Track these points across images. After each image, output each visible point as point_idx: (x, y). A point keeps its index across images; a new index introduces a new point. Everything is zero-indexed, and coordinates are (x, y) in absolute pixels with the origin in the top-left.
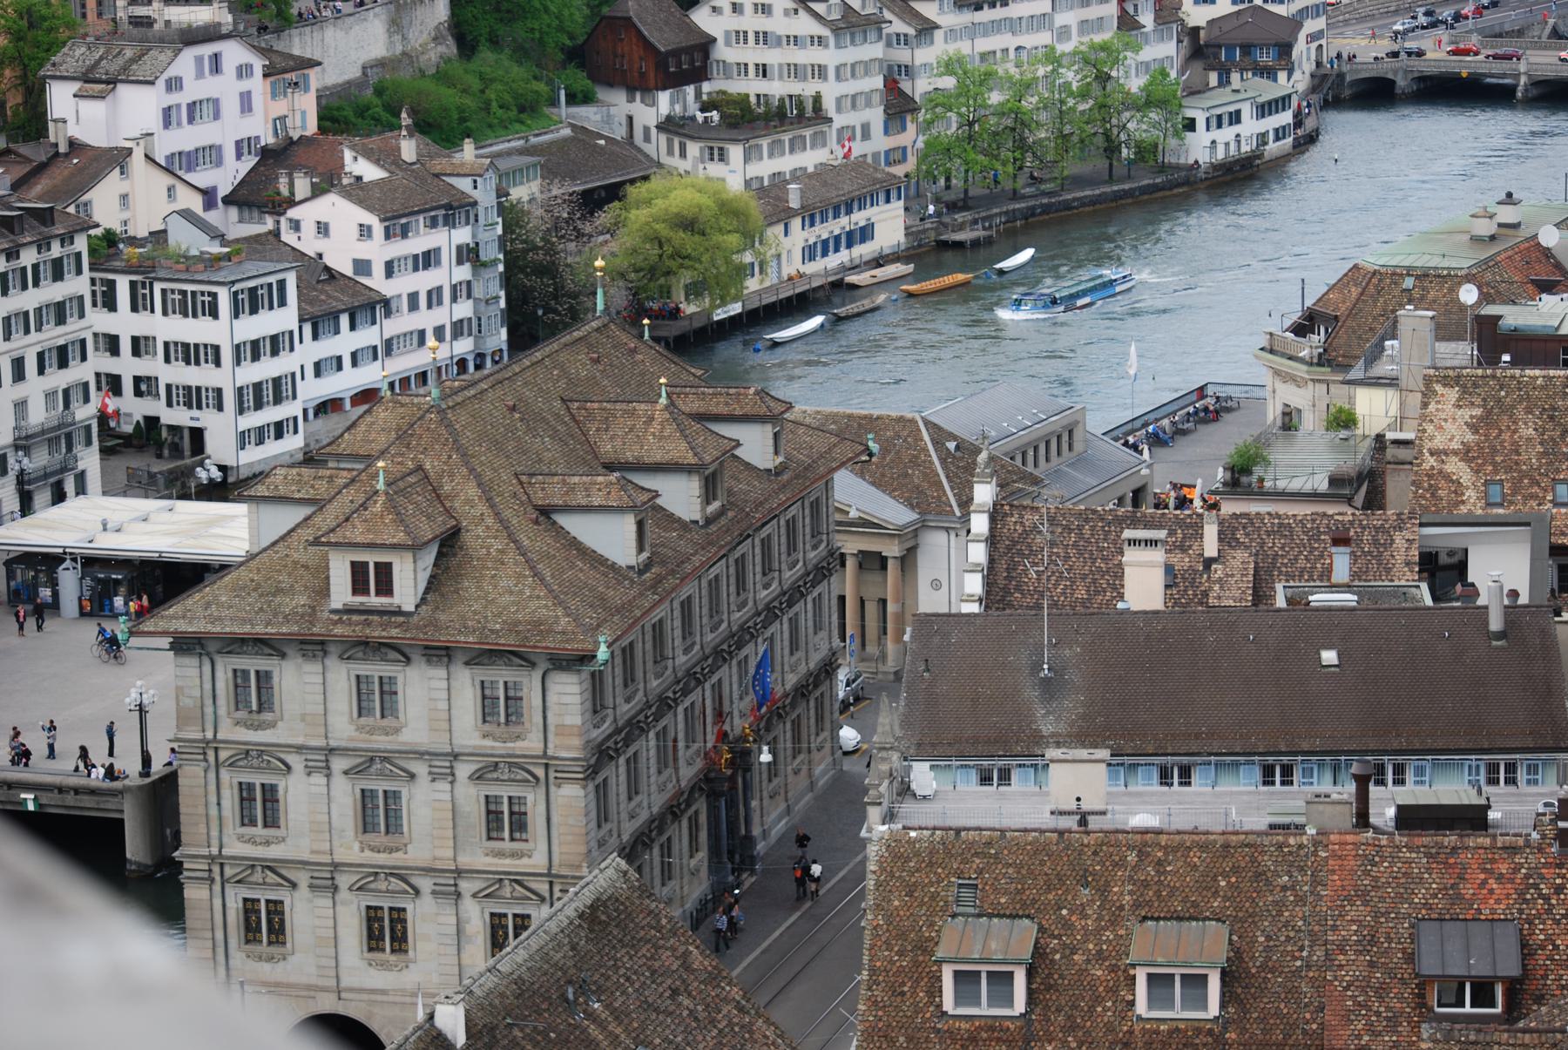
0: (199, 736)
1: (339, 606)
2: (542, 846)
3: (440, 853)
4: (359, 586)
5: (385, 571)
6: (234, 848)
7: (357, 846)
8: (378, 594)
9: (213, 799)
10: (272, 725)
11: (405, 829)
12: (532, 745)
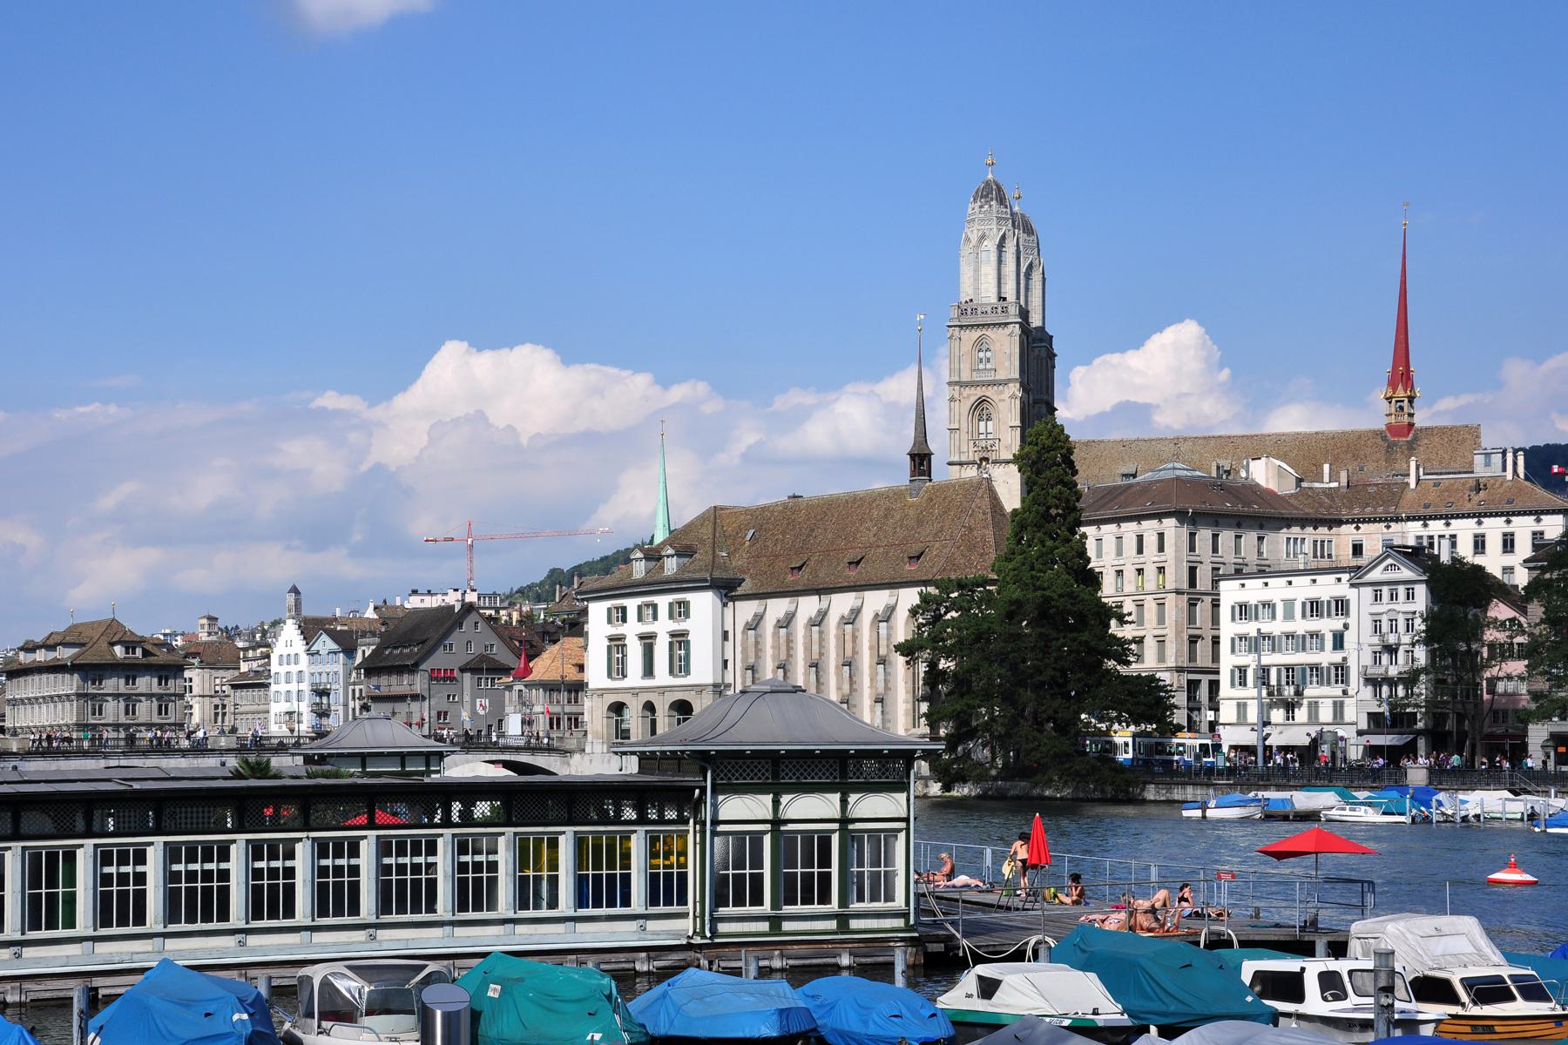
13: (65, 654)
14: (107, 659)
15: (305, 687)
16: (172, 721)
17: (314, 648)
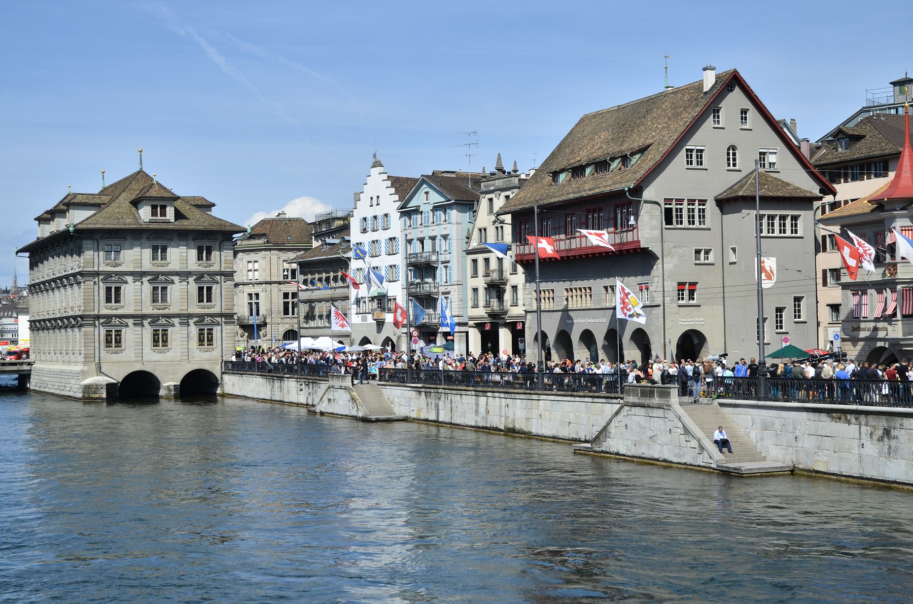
0: (91, 269)
2: (219, 304)
3: (182, 308)
4: (154, 214)
5: (163, 208)
6: (104, 311)
7: (151, 308)
9: (96, 293)
11: (169, 300)
13: (77, 217)
14: (128, 223)
15: (399, 260)
16: (216, 310)
17: (413, 204)
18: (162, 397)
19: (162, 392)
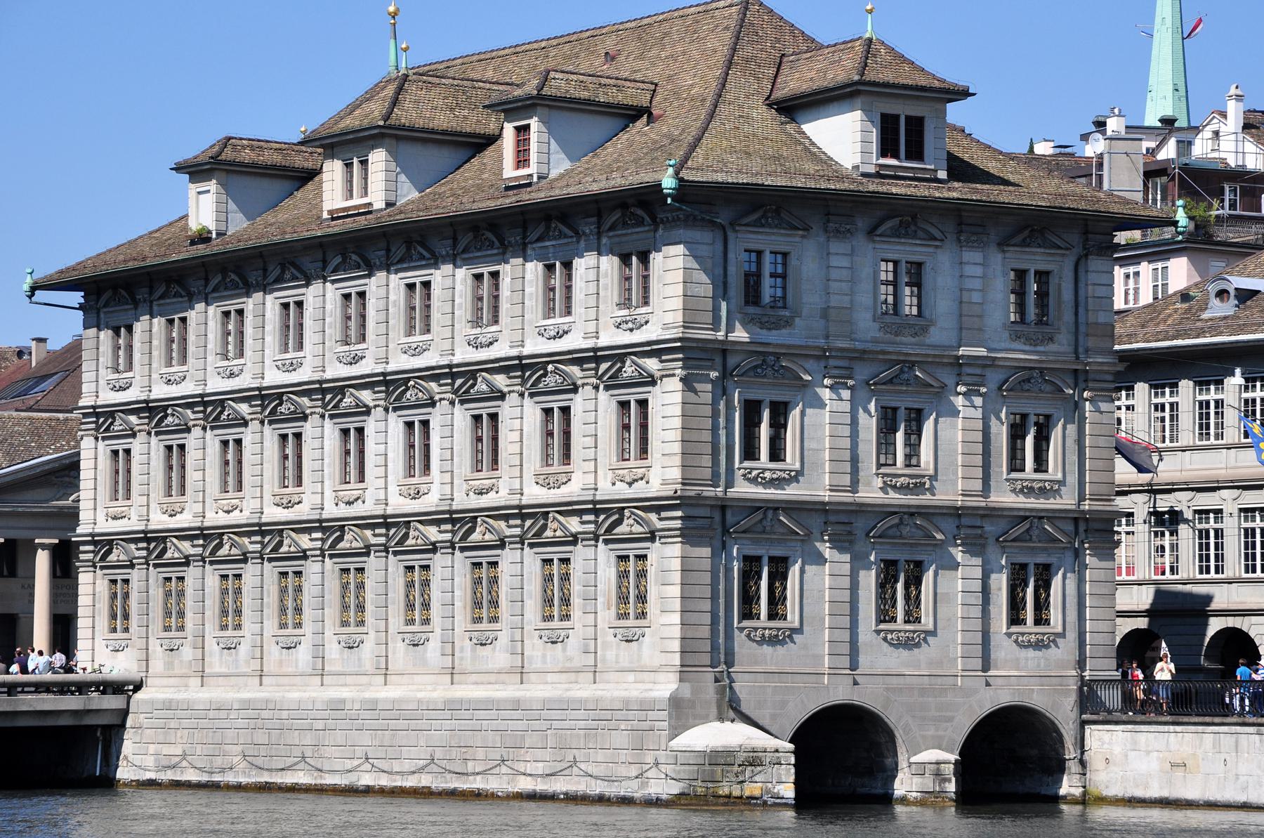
1: (872, 170)
2: (1072, 479)
4: (888, 146)
6: (743, 489)
7: (879, 482)
8: (909, 157)
9: (722, 421)
10: (788, 323)
12: (1062, 349)
16: (1066, 501)
18: (904, 800)
19: (905, 785)
